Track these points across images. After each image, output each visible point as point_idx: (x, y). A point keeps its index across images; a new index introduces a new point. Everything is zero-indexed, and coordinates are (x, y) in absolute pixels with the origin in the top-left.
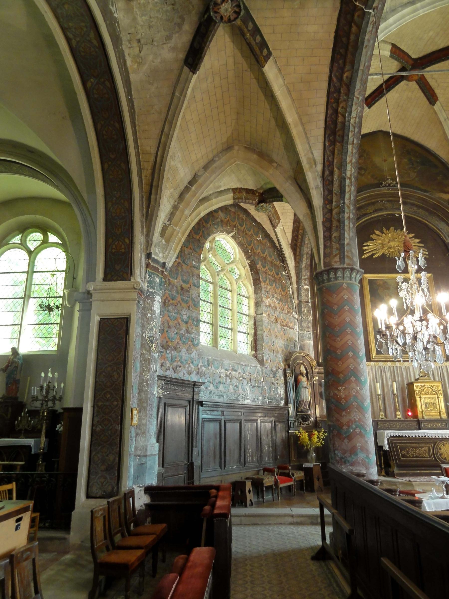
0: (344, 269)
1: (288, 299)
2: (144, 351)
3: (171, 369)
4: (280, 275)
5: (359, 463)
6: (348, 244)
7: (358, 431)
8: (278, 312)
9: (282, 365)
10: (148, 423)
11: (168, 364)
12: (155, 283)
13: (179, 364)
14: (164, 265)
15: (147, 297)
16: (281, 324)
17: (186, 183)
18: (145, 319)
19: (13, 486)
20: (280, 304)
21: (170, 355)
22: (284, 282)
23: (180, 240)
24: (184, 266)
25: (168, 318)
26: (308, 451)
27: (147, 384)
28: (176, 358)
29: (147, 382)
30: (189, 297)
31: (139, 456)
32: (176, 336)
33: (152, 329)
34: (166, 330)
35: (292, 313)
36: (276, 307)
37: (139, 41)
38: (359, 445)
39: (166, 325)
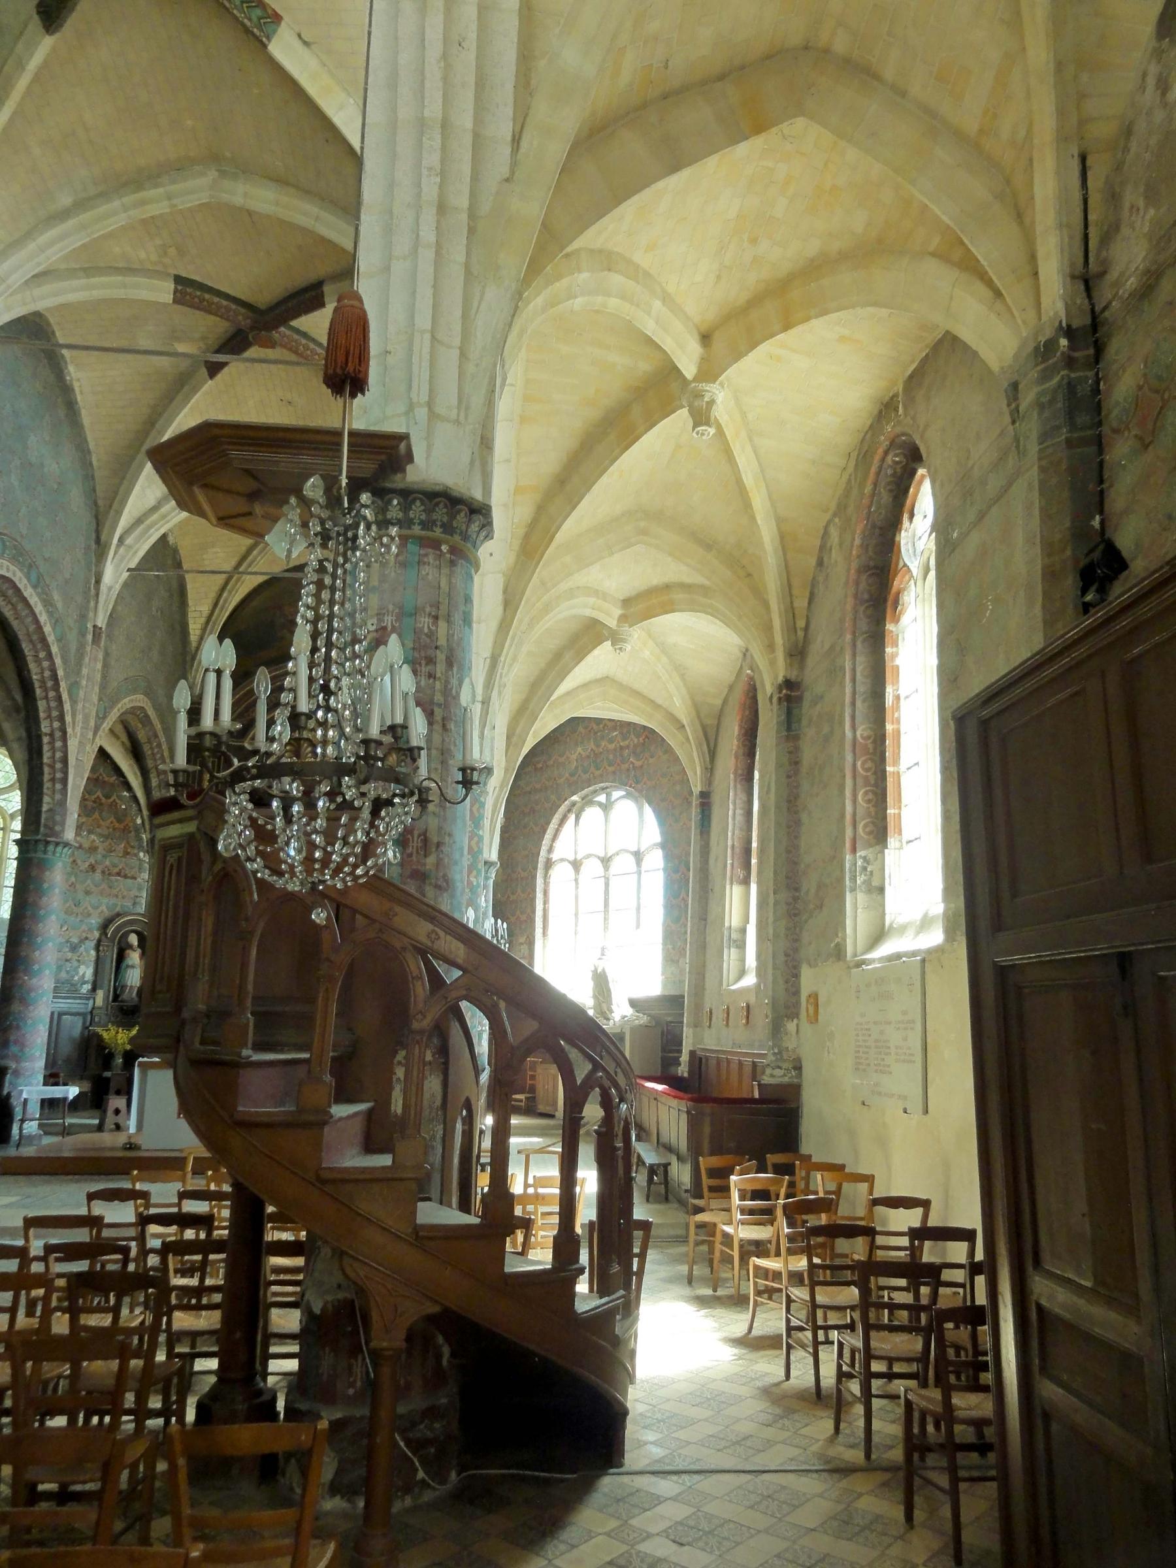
0: (37, 841)
1: (130, 832)
4: (114, 797)
6: (50, 810)
7: (15, 1023)
8: (99, 857)
9: (97, 934)
16: (103, 872)
20: (107, 843)
22: (124, 807)
26: (111, 1056)
35: (136, 855)
36: (96, 849)
38: (12, 1038)
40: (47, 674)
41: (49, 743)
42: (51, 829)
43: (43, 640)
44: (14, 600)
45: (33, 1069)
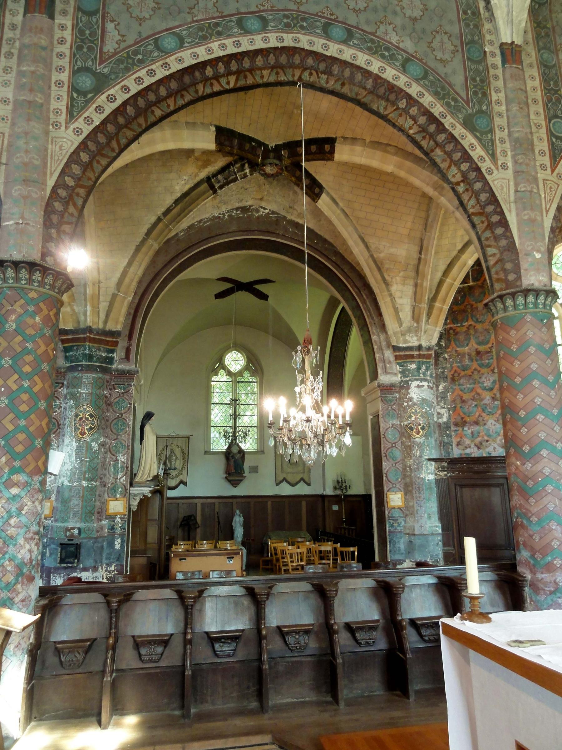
2: (404, 439)
3: (472, 446)
5: (522, 563)
10: (415, 505)
11: (467, 442)
12: (409, 370)
13: (486, 438)
14: (420, 347)
15: (402, 387)
17: (416, 256)
18: (402, 409)
19: (355, 549)
21: (470, 431)
23: (441, 309)
24: (479, 327)
25: (460, 393)
27: (411, 469)
28: (479, 433)
29: (410, 467)
30: (492, 358)
31: (408, 534)
32: (475, 409)
33: (410, 417)
34: (459, 406)
37: (290, 207)
39: (458, 401)
40: (422, 120)
41: (467, 190)
42: (506, 281)
43: (392, 88)
44: (322, 66)
45: (555, 582)
